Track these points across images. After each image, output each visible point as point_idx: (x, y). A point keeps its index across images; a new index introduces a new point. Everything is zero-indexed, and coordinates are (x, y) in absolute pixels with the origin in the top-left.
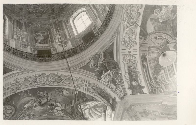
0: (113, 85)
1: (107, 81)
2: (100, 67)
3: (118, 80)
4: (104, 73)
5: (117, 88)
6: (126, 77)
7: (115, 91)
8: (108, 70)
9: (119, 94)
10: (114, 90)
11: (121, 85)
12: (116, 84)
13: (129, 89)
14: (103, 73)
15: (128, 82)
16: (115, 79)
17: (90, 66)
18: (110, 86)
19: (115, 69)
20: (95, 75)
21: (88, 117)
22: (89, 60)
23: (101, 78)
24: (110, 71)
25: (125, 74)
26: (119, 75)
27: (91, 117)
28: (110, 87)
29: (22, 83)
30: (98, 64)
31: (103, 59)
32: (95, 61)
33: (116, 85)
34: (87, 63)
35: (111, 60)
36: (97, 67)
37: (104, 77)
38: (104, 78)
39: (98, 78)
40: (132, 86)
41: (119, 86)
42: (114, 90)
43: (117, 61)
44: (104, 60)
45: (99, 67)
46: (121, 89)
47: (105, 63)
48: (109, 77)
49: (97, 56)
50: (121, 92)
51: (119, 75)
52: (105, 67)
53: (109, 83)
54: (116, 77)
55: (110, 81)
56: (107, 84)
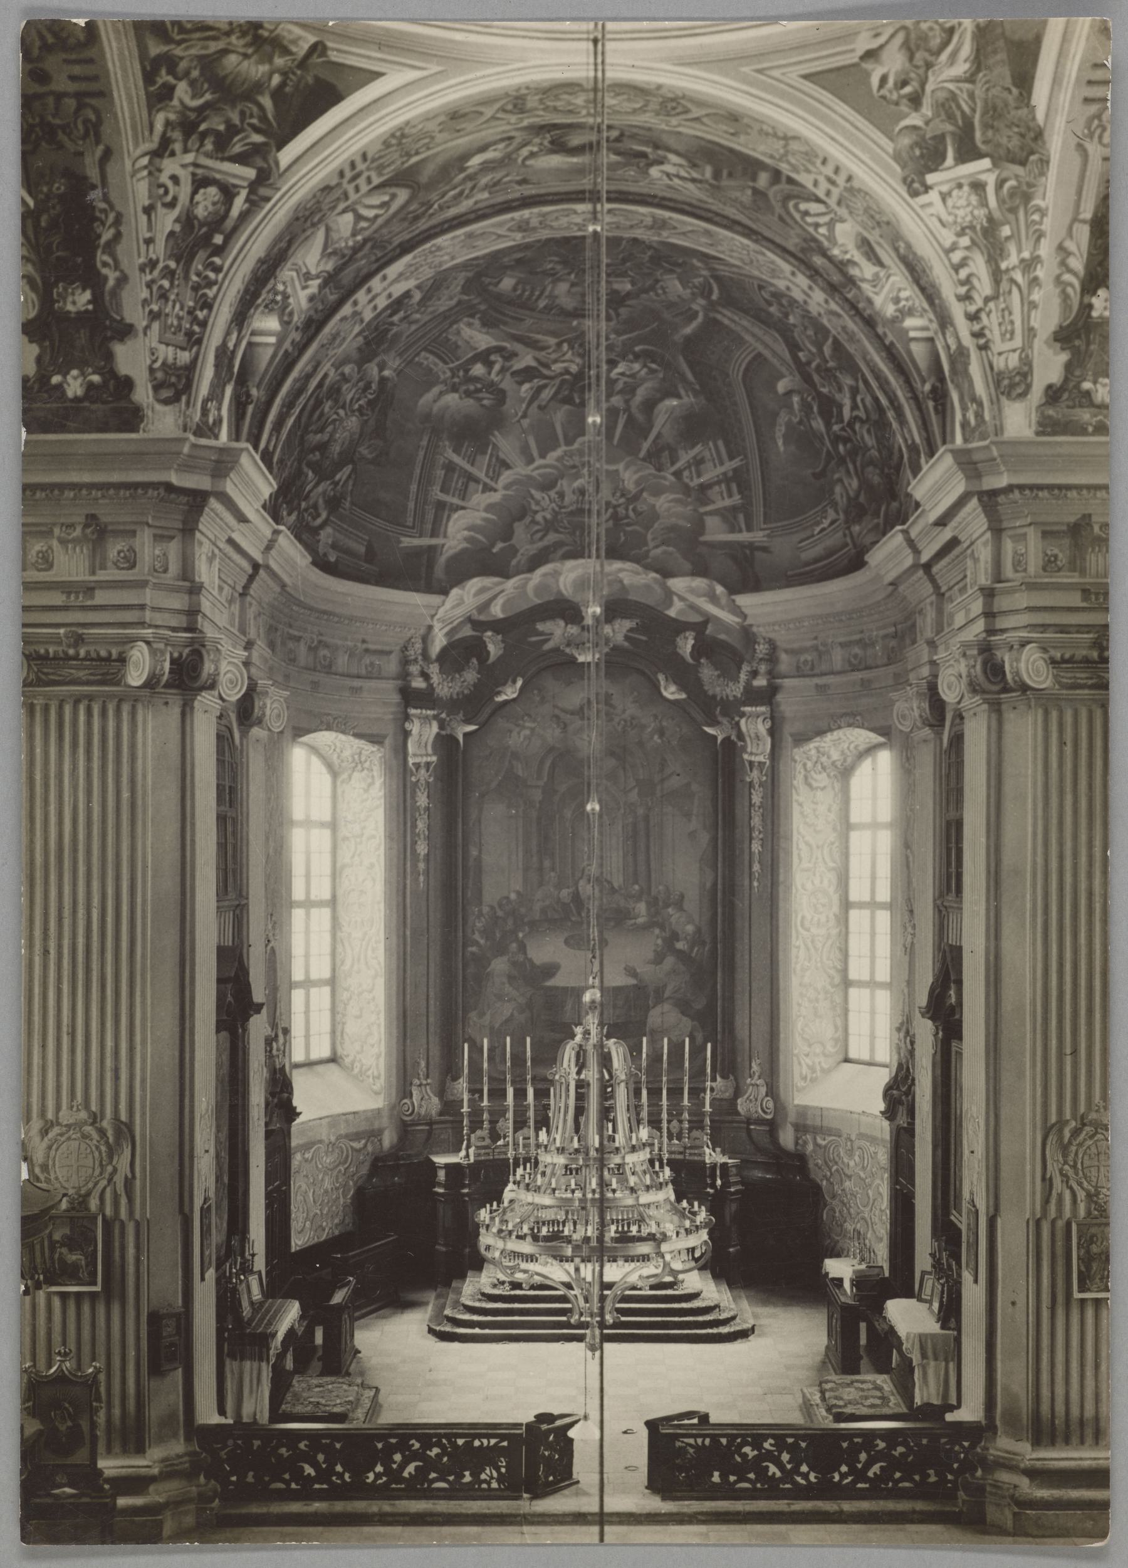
0: (979, 266)
1: (955, 222)
2: (936, 115)
3: (1020, 251)
4: (950, 160)
5: (995, 297)
6: (1069, 254)
7: (979, 311)
8: (980, 156)
9: (998, 346)
10: (980, 303)
11: (1025, 291)
12: (998, 267)
13: (1058, 345)
14: (943, 157)
15: (1069, 290)
16: (1006, 231)
17: (875, 81)
18: (963, 263)
19: (1019, 170)
20: (891, 151)
21: (848, 256)
22: (877, 35)
23: (927, 188)
24: (986, 163)
25: (1063, 232)
26: (1036, 217)
27: (869, 259)
28: (963, 273)
29: (438, 129)
30: (929, 87)
31: (967, 66)
32: (911, 58)
33: (997, 276)
34: (860, 52)
35: (1011, 99)
36: (915, 101)
37: (945, 188)
38: (944, 197)
39: (904, 180)
40: (1080, 324)
41: (1010, 292)
42: (980, 303)
43: (1047, 115)
44: (971, 79)
45: (927, 110)
46: (1017, 318)
47: (972, 95)
48: (974, 199)
49: (931, 29)
50: (1011, 339)
51: (1036, 217)
52: (968, 128)
53: (965, 241)
54: (1011, 217)
55: (972, 227)
56: (947, 237)
